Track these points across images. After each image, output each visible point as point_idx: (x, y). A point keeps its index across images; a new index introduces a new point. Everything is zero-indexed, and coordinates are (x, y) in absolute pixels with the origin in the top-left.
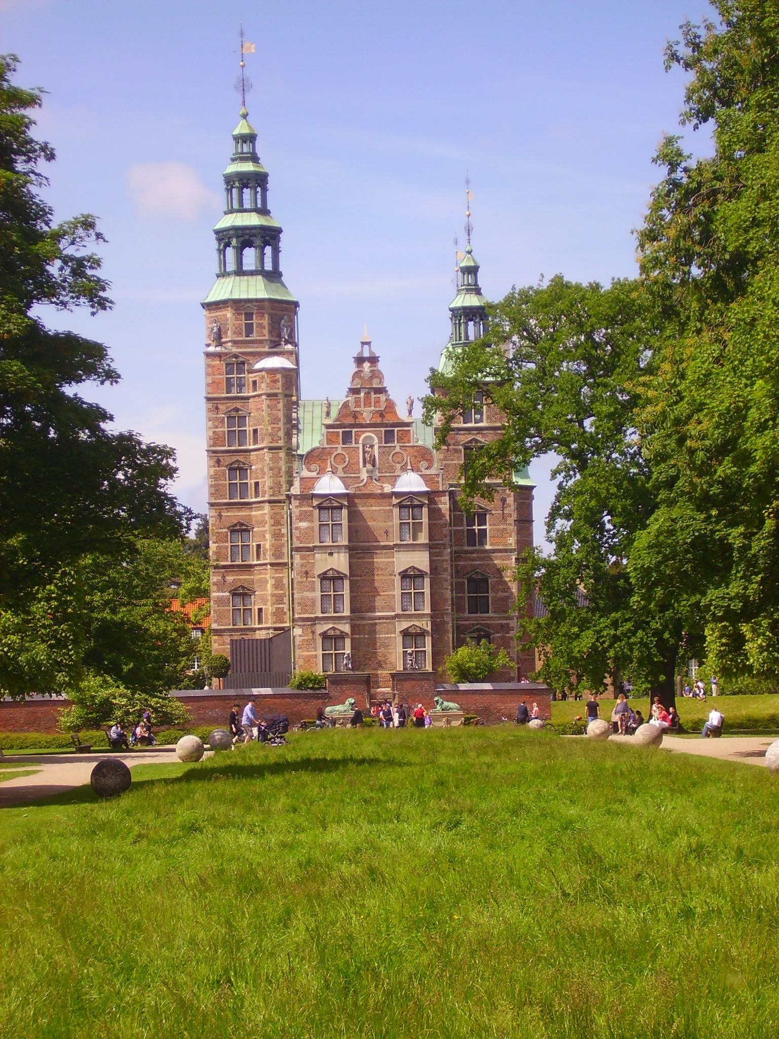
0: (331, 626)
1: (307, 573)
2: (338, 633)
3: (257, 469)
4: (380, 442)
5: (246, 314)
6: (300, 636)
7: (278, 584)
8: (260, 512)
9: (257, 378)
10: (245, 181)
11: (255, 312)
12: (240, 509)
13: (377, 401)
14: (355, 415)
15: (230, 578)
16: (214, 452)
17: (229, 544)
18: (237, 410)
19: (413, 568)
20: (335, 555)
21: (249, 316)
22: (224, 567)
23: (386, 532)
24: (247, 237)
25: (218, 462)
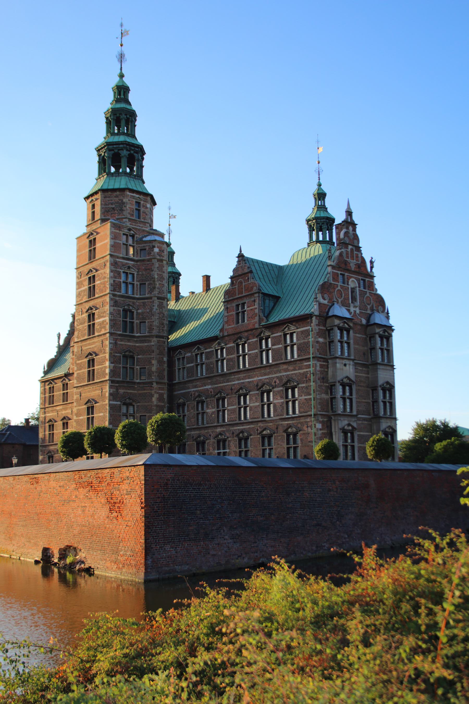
0: (346, 422)
1: (323, 378)
2: (350, 428)
3: (143, 313)
4: (359, 287)
5: (136, 202)
6: (321, 430)
7: (160, 399)
8: (146, 344)
9: (147, 248)
10: (128, 116)
11: (142, 202)
12: (129, 341)
13: (357, 257)
14: (346, 263)
15: (121, 391)
16: (114, 295)
17: (121, 365)
18: (129, 268)
19: (388, 383)
20: (347, 366)
21: (138, 203)
22: (118, 382)
23: (364, 354)
24: (132, 152)
25: (116, 302)
